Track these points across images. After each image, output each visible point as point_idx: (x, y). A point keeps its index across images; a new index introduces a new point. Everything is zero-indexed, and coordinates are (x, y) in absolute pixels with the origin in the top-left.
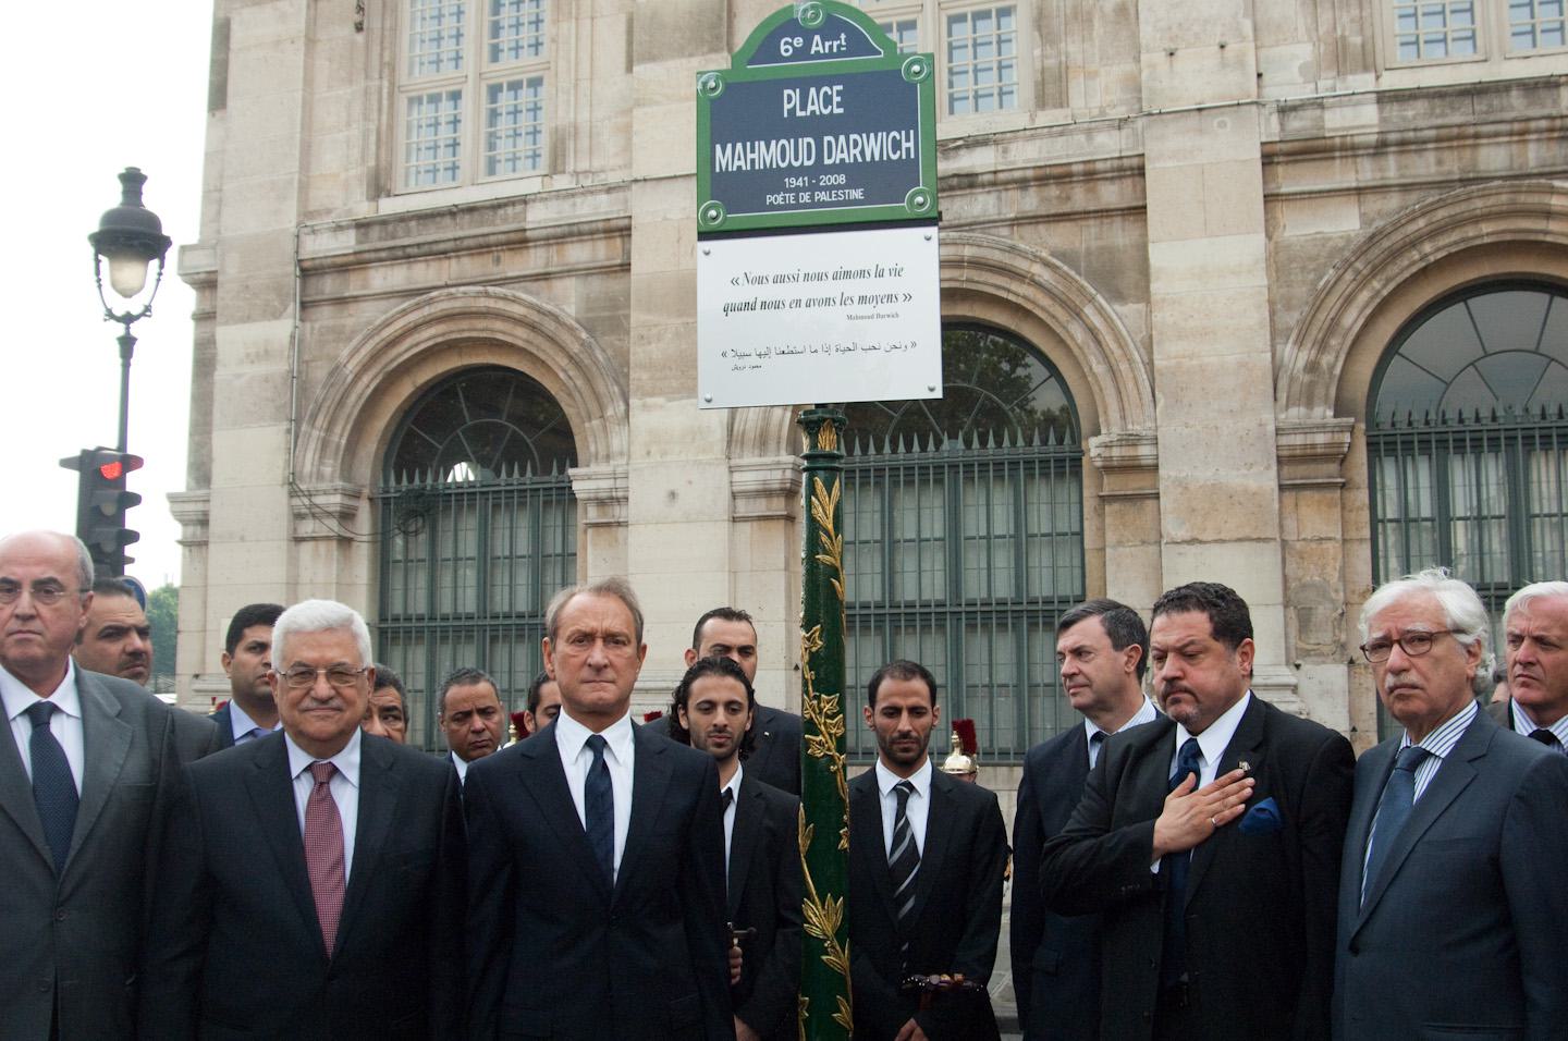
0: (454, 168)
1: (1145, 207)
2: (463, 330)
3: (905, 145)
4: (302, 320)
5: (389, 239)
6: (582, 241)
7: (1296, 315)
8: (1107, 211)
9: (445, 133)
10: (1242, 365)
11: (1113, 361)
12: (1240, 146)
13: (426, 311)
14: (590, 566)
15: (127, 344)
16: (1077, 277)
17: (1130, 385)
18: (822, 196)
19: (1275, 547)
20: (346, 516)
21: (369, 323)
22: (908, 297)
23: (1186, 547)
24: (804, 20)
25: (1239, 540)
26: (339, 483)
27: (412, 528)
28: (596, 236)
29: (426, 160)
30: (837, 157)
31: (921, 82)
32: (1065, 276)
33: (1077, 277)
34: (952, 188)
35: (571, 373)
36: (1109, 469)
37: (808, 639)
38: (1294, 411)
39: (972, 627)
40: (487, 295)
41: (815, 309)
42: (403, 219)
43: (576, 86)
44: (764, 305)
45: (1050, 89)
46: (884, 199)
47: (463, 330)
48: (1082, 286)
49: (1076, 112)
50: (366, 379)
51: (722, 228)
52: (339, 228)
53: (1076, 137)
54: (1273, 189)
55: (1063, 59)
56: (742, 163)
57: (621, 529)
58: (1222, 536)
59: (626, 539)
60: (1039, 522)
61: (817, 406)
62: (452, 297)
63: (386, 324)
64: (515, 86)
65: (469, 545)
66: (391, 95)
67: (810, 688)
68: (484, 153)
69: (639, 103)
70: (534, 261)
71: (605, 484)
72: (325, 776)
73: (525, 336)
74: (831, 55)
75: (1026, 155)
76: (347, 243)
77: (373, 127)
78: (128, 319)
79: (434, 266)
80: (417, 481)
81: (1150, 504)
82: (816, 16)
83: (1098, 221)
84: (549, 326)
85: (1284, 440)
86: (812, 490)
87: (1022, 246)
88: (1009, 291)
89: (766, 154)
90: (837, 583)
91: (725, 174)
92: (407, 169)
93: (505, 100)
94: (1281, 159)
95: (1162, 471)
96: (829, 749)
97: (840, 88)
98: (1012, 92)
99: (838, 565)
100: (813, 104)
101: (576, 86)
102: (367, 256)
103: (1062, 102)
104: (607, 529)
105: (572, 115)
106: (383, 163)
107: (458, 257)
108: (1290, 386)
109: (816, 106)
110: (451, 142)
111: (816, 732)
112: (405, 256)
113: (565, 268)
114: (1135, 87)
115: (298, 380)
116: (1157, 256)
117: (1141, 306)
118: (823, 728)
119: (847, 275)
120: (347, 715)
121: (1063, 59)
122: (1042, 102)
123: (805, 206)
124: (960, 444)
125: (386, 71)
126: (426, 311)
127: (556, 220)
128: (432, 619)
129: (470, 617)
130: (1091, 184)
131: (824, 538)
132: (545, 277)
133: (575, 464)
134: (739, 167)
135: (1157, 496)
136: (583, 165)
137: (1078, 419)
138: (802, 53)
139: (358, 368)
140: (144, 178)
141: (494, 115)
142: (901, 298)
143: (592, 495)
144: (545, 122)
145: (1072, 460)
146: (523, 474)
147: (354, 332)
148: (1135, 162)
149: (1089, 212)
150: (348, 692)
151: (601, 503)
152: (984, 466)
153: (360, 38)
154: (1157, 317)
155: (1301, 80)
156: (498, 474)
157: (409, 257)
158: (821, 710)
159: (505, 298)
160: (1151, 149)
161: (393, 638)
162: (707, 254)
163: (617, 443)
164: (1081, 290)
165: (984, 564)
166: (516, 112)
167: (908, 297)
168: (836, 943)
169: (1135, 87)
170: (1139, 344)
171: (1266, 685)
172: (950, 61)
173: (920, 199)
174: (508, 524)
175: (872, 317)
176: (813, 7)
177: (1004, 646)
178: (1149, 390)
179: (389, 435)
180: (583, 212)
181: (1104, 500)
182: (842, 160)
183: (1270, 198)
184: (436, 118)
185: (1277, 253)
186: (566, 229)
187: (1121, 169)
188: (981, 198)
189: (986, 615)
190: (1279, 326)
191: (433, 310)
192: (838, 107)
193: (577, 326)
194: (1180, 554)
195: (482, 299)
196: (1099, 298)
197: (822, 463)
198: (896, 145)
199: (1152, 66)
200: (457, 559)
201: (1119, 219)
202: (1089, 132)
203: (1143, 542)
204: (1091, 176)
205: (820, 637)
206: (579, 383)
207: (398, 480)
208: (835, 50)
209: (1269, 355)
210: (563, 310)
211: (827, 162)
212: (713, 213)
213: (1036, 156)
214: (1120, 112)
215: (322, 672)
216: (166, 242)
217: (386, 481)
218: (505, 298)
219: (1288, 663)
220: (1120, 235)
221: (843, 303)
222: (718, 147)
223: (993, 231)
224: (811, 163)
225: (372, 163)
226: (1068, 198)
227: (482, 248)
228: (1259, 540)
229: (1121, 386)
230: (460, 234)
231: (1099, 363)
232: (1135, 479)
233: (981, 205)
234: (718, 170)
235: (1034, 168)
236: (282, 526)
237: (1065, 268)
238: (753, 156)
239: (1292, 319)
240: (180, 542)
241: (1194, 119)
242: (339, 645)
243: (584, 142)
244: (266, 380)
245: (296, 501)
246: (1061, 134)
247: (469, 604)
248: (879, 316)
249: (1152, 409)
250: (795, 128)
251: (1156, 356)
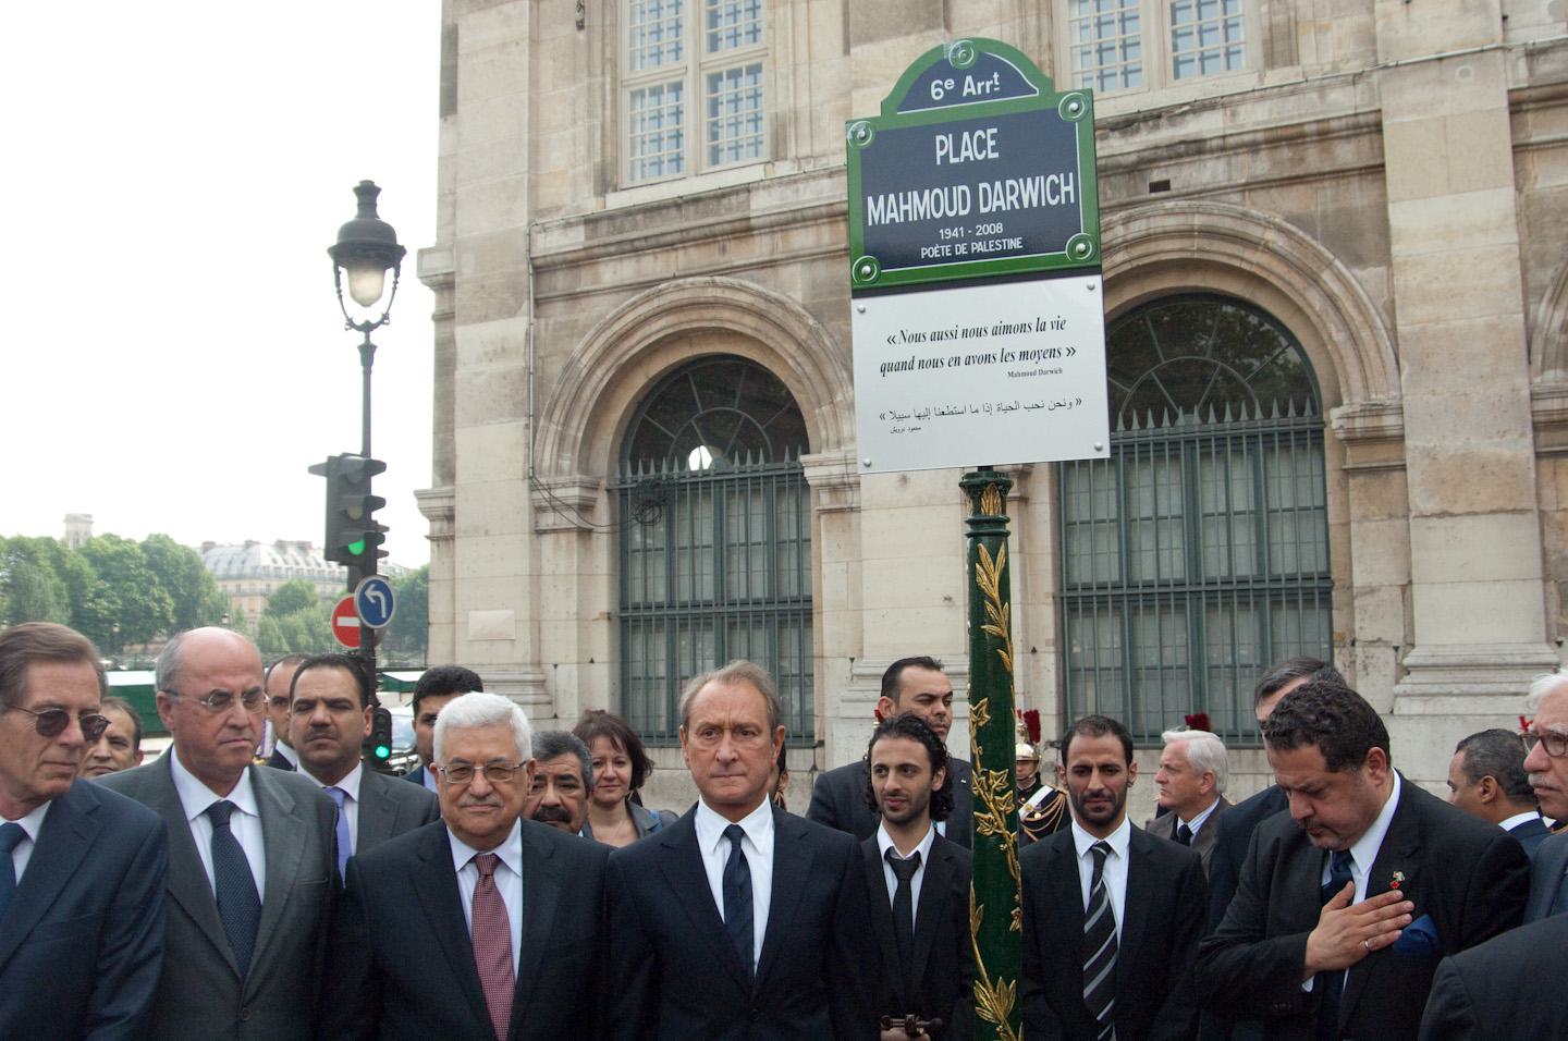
0: (678, 159)
1: (1383, 165)
2: (692, 321)
3: (1064, 189)
4: (535, 316)
5: (617, 234)
6: (807, 227)
7: (1550, 272)
8: (1343, 171)
9: (668, 125)
10: (1491, 327)
11: (1353, 328)
12: (1481, 99)
13: (656, 303)
14: (824, 552)
15: (367, 352)
16: (1314, 243)
17: (1373, 353)
18: (979, 247)
19: (1533, 518)
20: (585, 508)
21: (600, 317)
22: (1072, 351)
23: (1434, 522)
24: (955, 60)
25: (1493, 512)
26: (577, 476)
27: (649, 518)
28: (819, 221)
29: (650, 153)
30: (994, 204)
31: (1079, 120)
32: (1301, 242)
33: (1314, 243)
34: (1179, 156)
35: (799, 360)
36: (1352, 441)
37: (976, 713)
38: (1550, 375)
39: (1212, 605)
40: (715, 285)
41: (974, 367)
42: (629, 213)
43: (794, 72)
44: (922, 364)
45: (1279, 46)
46: (1038, 251)
47: (692, 321)
48: (1319, 251)
49: (1307, 69)
50: (599, 373)
51: (878, 284)
52: (568, 225)
53: (1308, 96)
54: (1522, 138)
55: (1292, 14)
56: (895, 215)
57: (854, 515)
58: (1476, 508)
59: (859, 524)
60: (1282, 494)
61: (980, 468)
62: (680, 288)
63: (618, 317)
64: (735, 75)
65: (706, 535)
66: (614, 90)
67: (979, 764)
68: (706, 143)
69: (857, 86)
70: (760, 248)
71: (837, 470)
72: (488, 866)
73: (753, 325)
74: (984, 96)
75: (1256, 117)
76: (576, 239)
77: (597, 122)
78: (368, 328)
79: (662, 258)
80: (652, 471)
81: (1396, 474)
82: (968, 55)
83: (1334, 183)
84: (776, 313)
85: (1541, 406)
86: (974, 558)
87: (1254, 212)
88: (1242, 259)
89: (920, 205)
90: (1004, 654)
91: (879, 227)
92: (632, 162)
93: (726, 89)
94: (1531, 106)
95: (1408, 442)
96: (998, 828)
97: (995, 131)
98: (1239, 52)
99: (1005, 635)
100: (967, 149)
101: (794, 72)
102: (596, 251)
103: (1292, 59)
104: (840, 515)
105: (792, 101)
106: (609, 159)
107: (684, 248)
108: (1545, 348)
109: (969, 152)
110: (674, 133)
111: (986, 810)
112: (633, 249)
113: (790, 255)
114: (1368, 38)
115: (535, 377)
116: (1398, 216)
117: (1382, 270)
118: (992, 805)
119: (1007, 329)
120: (505, 811)
121: (1292, 14)
122: (1271, 60)
124: (1196, 418)
125: (608, 67)
126: (656, 303)
127: (780, 207)
128: (671, 606)
129: (707, 605)
130: (1326, 144)
131: (990, 607)
132: (771, 264)
133: (806, 451)
134: (893, 220)
135: (1403, 468)
136: (805, 150)
137: (1320, 396)
138: (953, 96)
139: (592, 362)
140: (378, 190)
141: (714, 106)
142: (1064, 352)
143: (824, 482)
144: (767, 110)
145: (1313, 431)
146: (755, 460)
147: (587, 327)
148: (1372, 118)
149: (1324, 174)
150: (505, 788)
151: (834, 489)
152: (1221, 440)
153: (582, 36)
154: (1399, 281)
155: (1550, 20)
156: (733, 462)
157: (637, 250)
158: (989, 787)
159: (732, 287)
160: (1388, 104)
161: (633, 627)
162: (863, 312)
163: (846, 430)
164: (1318, 255)
165: (1223, 541)
166: (736, 100)
167: (1072, 351)
168: (1008, 1027)
169: (1368, 38)
170: (1381, 310)
171: (1525, 664)
172: (1174, 22)
173: (1081, 246)
174: (742, 512)
175: (1034, 374)
176: (963, 46)
177: (1247, 624)
178: (1393, 356)
179: (625, 425)
180: (807, 197)
181: (1349, 473)
182: (999, 208)
183: (1519, 149)
184: (659, 111)
185: (1528, 207)
186: (790, 216)
187: (1357, 126)
188: (1210, 164)
189: (1227, 594)
190: (1532, 284)
191: (662, 302)
192: (993, 151)
193: (803, 311)
194: (1430, 528)
195: (710, 290)
196: (1338, 263)
197: (986, 529)
198: (1055, 190)
199: (1387, 16)
200: (694, 547)
201: (1355, 182)
202: (1322, 90)
203: (1390, 516)
204: (1325, 135)
205: (988, 712)
206: (809, 369)
207: (635, 472)
208: (988, 91)
209: (1521, 316)
210: (789, 297)
211: (983, 210)
212: (867, 269)
213: (1266, 117)
214: (1355, 66)
215: (479, 768)
216: (401, 251)
217: (623, 474)
218: (732, 287)
219: (1548, 641)
220: (1358, 196)
221: (1004, 359)
222: (870, 199)
223: (1225, 198)
224: (966, 212)
225: (598, 159)
226: (1302, 160)
227: (708, 238)
228: (1514, 511)
229: (1363, 354)
230: (685, 225)
231: (1339, 331)
232: (1380, 451)
233: (1210, 171)
234: (870, 223)
235: (1266, 130)
236: (523, 520)
237: (1301, 233)
238: (906, 207)
239: (1546, 276)
240: (428, 537)
241: (1433, 72)
242: (496, 740)
243: (804, 128)
244: (504, 378)
245: (536, 495)
246: (1292, 93)
247: (707, 592)
248: (1042, 372)
249: (1396, 377)
250: (950, 176)
251: (1400, 322)
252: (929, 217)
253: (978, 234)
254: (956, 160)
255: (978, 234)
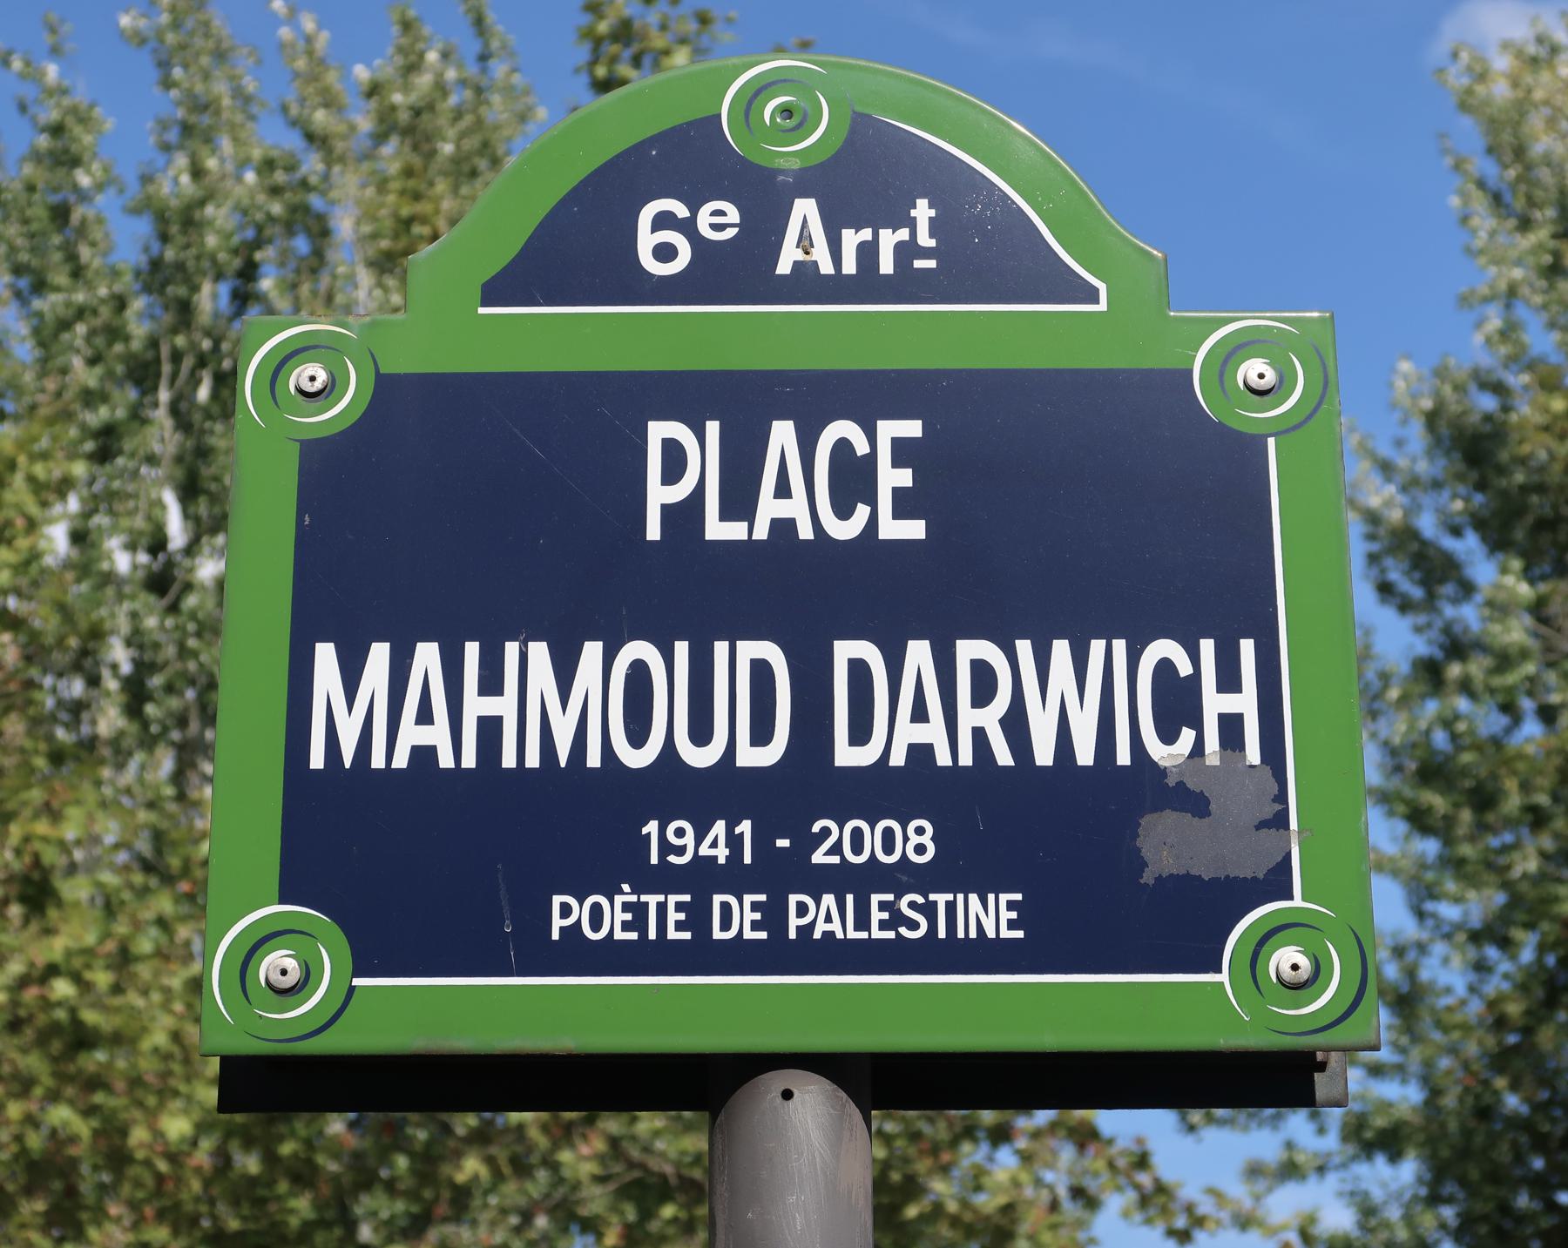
3: (1214, 703)
18: (824, 916)
30: (898, 737)
31: (1286, 429)
56: (437, 735)
74: (866, 284)
89: (556, 703)
97: (912, 428)
100: (783, 490)
109: (793, 502)
123: (738, 957)
138: (733, 271)
173: (1287, 958)
182: (921, 753)
192: (898, 514)
198: (1177, 703)
208: (886, 266)
211: (847, 755)
212: (278, 963)
222: (326, 656)
234: (317, 761)
250: (696, 592)
252: (594, 759)
253: (818, 857)
254: (735, 531)
255: (818, 857)
